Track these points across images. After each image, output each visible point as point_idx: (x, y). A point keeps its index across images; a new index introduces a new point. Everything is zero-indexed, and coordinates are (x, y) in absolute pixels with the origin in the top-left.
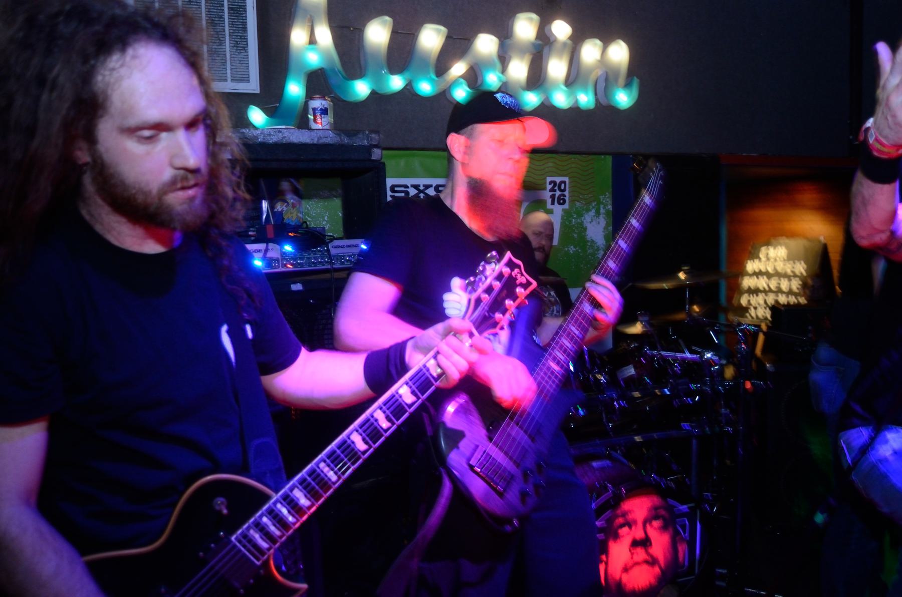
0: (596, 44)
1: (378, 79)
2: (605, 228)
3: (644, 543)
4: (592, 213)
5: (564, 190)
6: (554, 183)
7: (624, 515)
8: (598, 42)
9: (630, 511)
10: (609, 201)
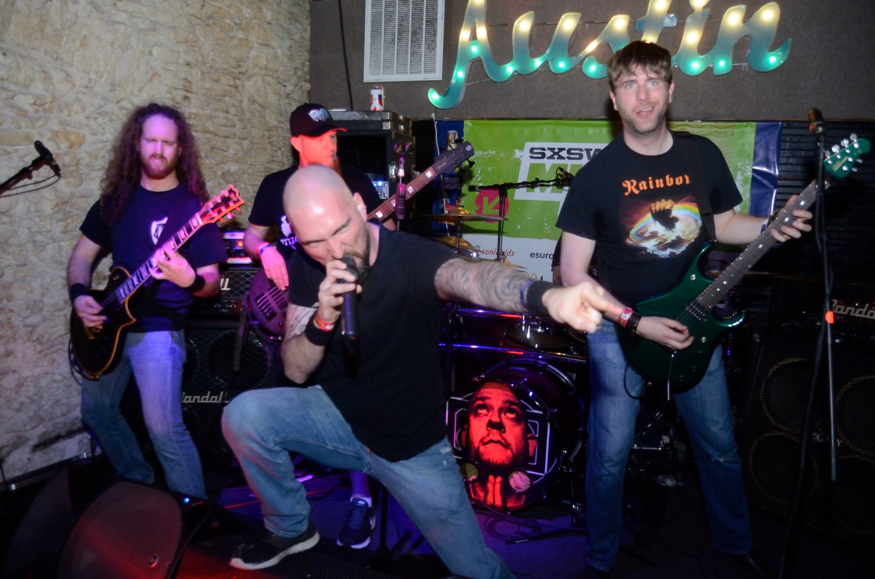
0: (740, 9)
1: (523, 62)
3: (499, 426)
7: (484, 399)
9: (490, 398)
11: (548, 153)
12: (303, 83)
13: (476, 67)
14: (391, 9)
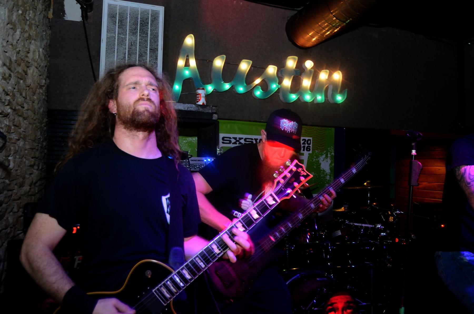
0: (327, 72)
2: (330, 164)
4: (324, 156)
5: (310, 144)
6: (305, 140)
8: (328, 71)
10: (333, 151)
11: (233, 141)
12: (47, 79)
13: (187, 83)
14: (123, 37)
